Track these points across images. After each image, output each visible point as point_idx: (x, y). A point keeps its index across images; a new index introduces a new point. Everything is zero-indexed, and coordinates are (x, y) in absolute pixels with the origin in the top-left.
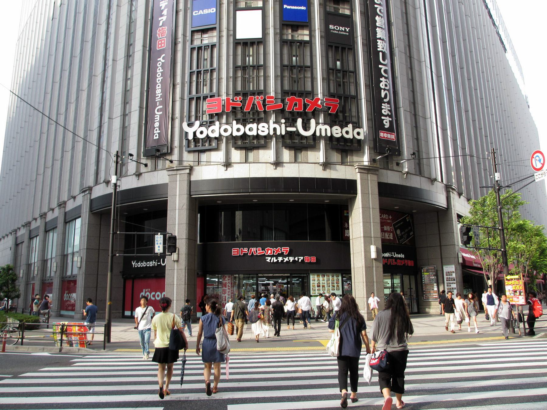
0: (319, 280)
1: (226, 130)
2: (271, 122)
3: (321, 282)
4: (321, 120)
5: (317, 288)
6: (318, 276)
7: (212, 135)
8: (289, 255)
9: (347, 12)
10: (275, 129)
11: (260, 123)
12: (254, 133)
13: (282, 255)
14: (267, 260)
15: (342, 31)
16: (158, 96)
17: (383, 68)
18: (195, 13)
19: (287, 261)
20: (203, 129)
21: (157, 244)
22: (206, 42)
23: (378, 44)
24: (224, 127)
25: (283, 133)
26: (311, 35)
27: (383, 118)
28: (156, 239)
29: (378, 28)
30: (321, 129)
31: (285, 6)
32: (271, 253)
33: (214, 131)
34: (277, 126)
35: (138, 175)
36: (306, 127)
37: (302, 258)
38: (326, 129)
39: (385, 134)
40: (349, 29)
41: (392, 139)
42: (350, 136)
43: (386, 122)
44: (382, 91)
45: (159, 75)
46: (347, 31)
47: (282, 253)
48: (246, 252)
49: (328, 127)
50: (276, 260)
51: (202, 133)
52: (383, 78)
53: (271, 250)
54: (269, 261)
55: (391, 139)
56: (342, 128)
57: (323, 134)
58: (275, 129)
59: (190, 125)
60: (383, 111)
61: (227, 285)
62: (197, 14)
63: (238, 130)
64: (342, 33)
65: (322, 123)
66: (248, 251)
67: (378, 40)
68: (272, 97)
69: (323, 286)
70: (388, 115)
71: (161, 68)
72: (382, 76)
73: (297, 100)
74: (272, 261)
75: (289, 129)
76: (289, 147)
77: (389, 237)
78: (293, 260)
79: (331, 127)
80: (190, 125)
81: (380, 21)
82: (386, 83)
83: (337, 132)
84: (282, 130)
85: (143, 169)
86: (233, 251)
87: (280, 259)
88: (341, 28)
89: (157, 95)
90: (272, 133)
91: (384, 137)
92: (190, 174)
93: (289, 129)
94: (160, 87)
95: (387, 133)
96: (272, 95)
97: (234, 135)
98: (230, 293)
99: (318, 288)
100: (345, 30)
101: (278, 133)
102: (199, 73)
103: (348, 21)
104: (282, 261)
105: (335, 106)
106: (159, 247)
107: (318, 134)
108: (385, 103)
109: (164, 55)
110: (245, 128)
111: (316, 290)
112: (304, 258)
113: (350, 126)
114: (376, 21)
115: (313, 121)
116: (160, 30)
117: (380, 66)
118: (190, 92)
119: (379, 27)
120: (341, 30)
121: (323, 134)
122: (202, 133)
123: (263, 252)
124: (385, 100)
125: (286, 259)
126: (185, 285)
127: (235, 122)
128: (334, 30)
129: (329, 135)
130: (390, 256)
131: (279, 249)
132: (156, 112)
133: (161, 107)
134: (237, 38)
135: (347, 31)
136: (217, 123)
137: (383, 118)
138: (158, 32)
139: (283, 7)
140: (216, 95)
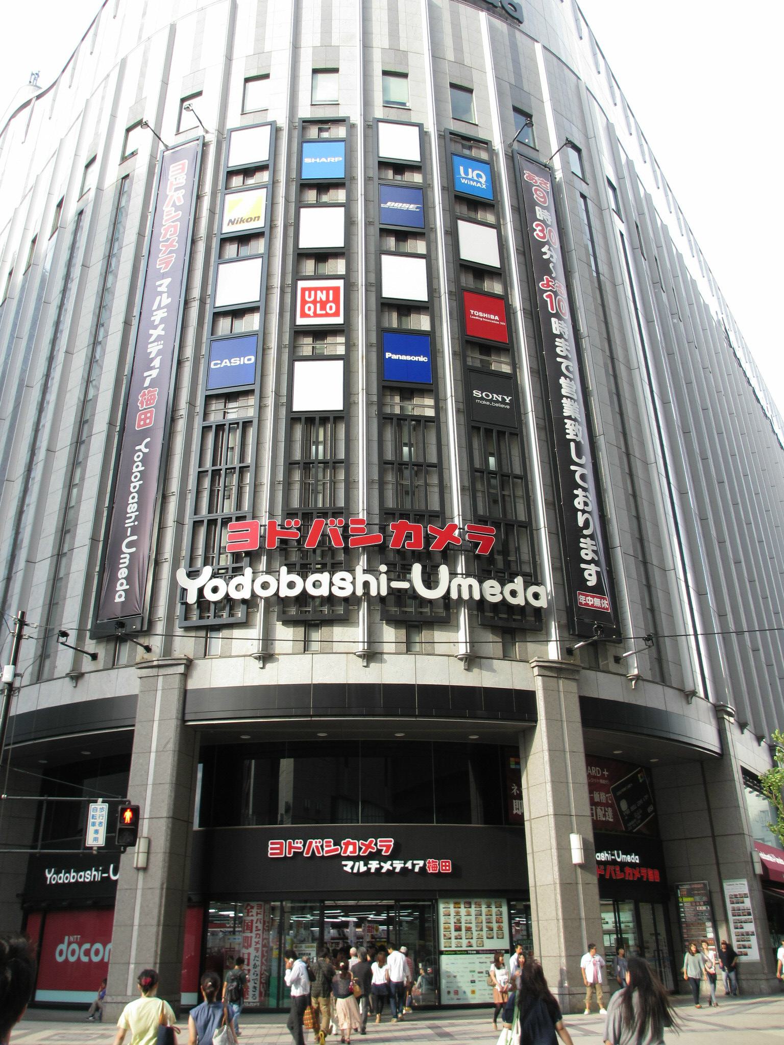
0: (458, 914)
1: (265, 586)
2: (359, 569)
3: (463, 919)
4: (461, 568)
5: (454, 934)
6: (457, 905)
8: (392, 857)
9: (506, 369)
10: (366, 585)
11: (337, 571)
12: (324, 591)
13: (376, 855)
14: (345, 868)
15: (497, 401)
16: (131, 517)
17: (579, 471)
18: (215, 364)
19: (388, 870)
21: (94, 824)
22: (232, 416)
25: (384, 592)
26: (439, 407)
27: (583, 566)
28: (91, 813)
29: (564, 398)
30: (460, 586)
31: (388, 355)
32: (354, 852)
34: (370, 578)
35: (76, 676)
36: (430, 581)
37: (421, 863)
38: (470, 586)
40: (510, 398)
41: (604, 608)
42: (519, 601)
43: (590, 575)
44: (579, 514)
45: (136, 477)
47: (379, 851)
48: (300, 848)
49: (474, 582)
51: (215, 590)
53: (354, 844)
54: (350, 871)
55: (601, 608)
56: (503, 585)
58: (366, 585)
59: (193, 574)
60: (583, 553)
61: (254, 925)
62: (219, 366)
63: (291, 585)
64: (497, 405)
65: (462, 574)
66: (304, 846)
67: (566, 421)
69: (468, 929)
72: (578, 486)
74: (355, 871)
75: (396, 585)
76: (395, 622)
77: (605, 815)
78: (402, 869)
79: (481, 582)
80: (193, 574)
81: (568, 386)
82: (586, 499)
83: (493, 591)
84: (380, 585)
85: (87, 664)
86: (270, 846)
87: (374, 865)
89: (128, 515)
90: (360, 592)
91: (587, 604)
92: (185, 676)
93: (396, 585)
94: (136, 500)
95: (593, 597)
96: (361, 517)
97: (282, 594)
98: (259, 946)
99: (457, 933)
101: (373, 592)
103: (510, 383)
106: (96, 832)
107: (454, 595)
108: (585, 537)
109: (148, 440)
110: (304, 581)
111: (453, 938)
112: (425, 865)
113: (519, 580)
114: (560, 387)
115: (444, 570)
116: (144, 395)
117: (573, 468)
118: (196, 511)
119: (567, 397)
120: (494, 399)
121: (466, 596)
122: (215, 590)
123: (337, 850)
124: (585, 532)
125: (387, 866)
126: (158, 925)
127: (284, 569)
128: (482, 399)
130: (609, 859)
132: (124, 549)
134: (295, 409)
135: (507, 401)
136: (248, 571)
137: (583, 566)
139: (385, 355)
140: (249, 516)
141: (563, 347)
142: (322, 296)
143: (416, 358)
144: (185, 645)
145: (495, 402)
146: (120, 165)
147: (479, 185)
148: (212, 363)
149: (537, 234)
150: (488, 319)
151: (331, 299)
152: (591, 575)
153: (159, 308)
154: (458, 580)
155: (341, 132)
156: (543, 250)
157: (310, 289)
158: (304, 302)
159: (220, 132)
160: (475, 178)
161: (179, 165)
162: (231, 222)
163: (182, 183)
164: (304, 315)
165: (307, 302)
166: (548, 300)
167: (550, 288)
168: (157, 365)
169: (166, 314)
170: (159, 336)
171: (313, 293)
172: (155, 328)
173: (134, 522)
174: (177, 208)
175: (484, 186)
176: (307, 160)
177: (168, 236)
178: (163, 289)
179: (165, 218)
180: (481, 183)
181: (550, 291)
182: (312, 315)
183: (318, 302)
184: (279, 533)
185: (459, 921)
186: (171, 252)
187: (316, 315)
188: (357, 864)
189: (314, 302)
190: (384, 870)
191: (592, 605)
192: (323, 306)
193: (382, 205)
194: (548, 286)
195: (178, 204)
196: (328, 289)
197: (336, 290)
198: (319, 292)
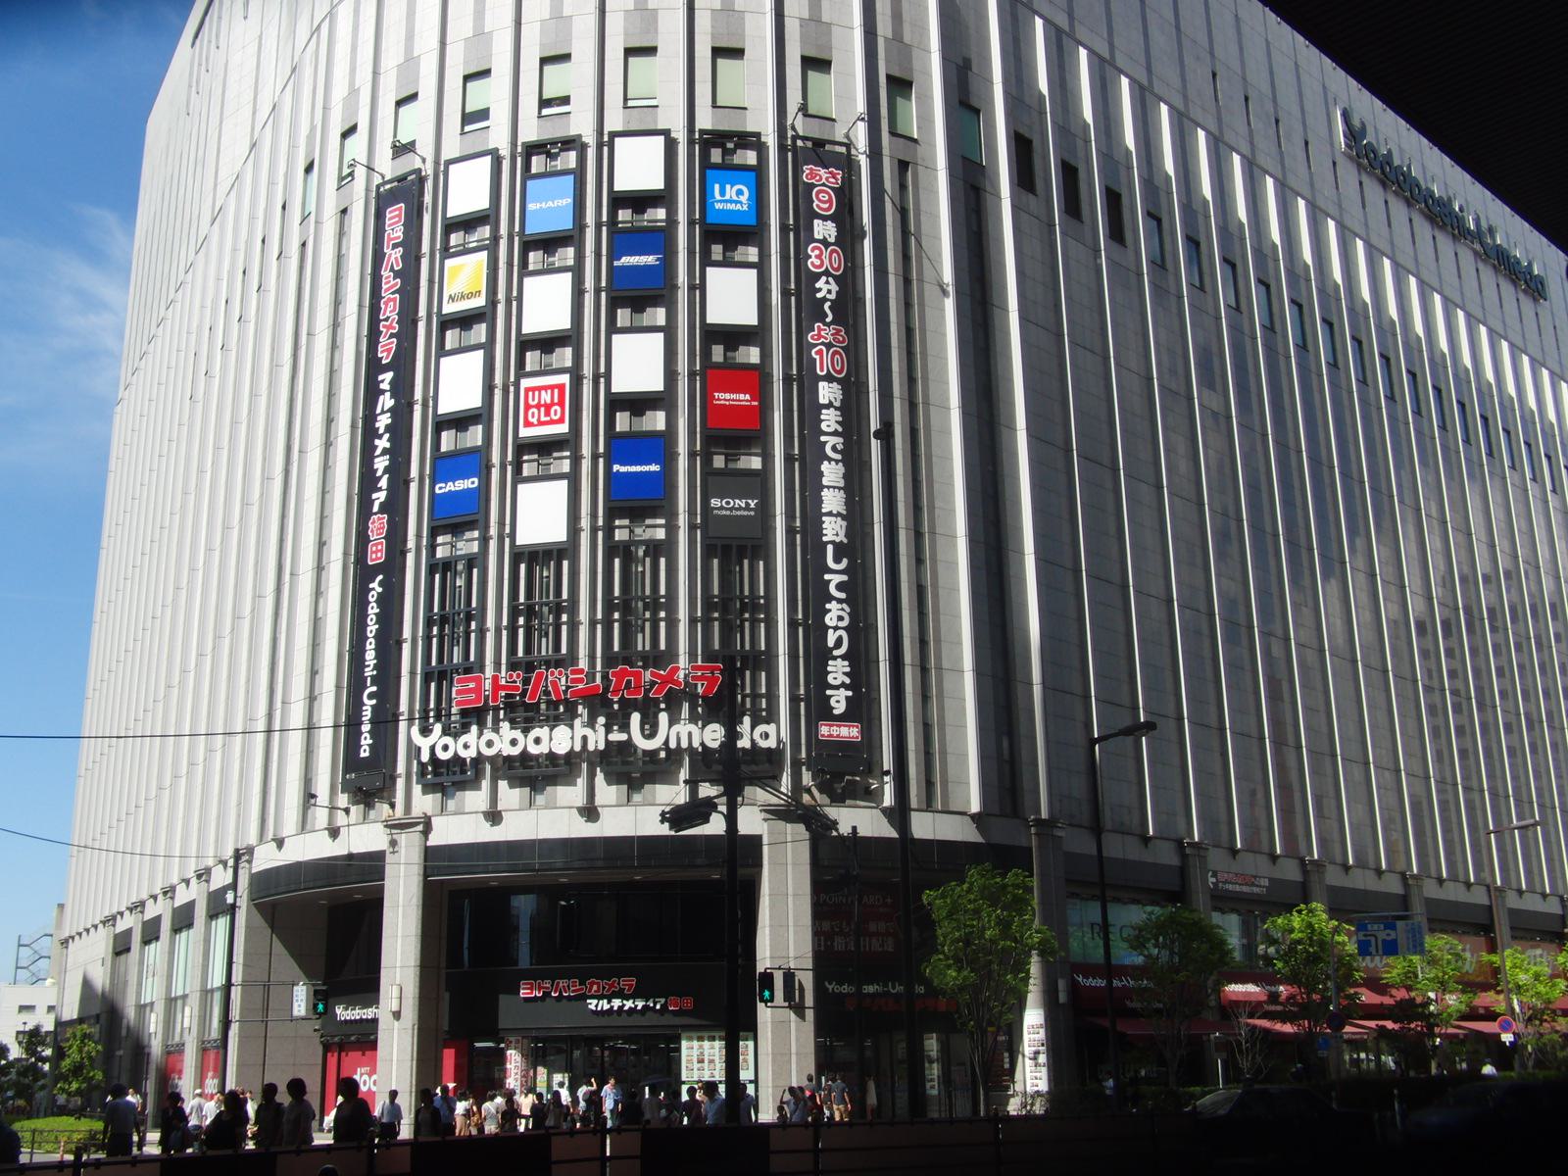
0: (701, 1047)
2: (577, 722)
3: (706, 1053)
5: (696, 1066)
7: (463, 754)
8: (633, 996)
9: (756, 463)
10: (585, 739)
12: (543, 749)
14: (590, 1006)
15: (740, 508)
16: (369, 666)
17: (834, 579)
18: (440, 488)
19: (630, 1008)
21: (297, 1001)
23: (824, 526)
24: (488, 735)
25: (602, 746)
29: (825, 490)
31: (616, 468)
33: (470, 744)
34: (588, 732)
35: (334, 832)
36: (650, 728)
38: (690, 734)
39: (835, 728)
40: (756, 501)
41: (853, 737)
43: (838, 702)
44: (831, 631)
45: (372, 620)
46: (752, 506)
47: (622, 990)
48: (548, 988)
50: (609, 1006)
51: (446, 748)
52: (834, 602)
53: (598, 984)
54: (594, 1009)
55: (850, 737)
57: (684, 744)
58: (585, 739)
59: (426, 731)
60: (830, 679)
61: (513, 1058)
62: (442, 491)
63: (514, 742)
64: (739, 513)
65: (685, 719)
66: (552, 986)
67: (824, 518)
68: (581, 671)
69: (711, 1061)
70: (843, 685)
71: (375, 605)
72: (831, 598)
74: (599, 1009)
76: (613, 778)
77: (882, 946)
78: (643, 1006)
80: (426, 731)
81: (832, 473)
82: (841, 613)
84: (597, 739)
86: (522, 986)
88: (737, 501)
89: (367, 663)
90: (578, 748)
91: (831, 736)
94: (373, 646)
95: (839, 726)
98: (519, 1077)
99: (700, 1065)
100: (747, 504)
101: (591, 747)
104: (621, 1008)
106: (299, 1006)
107: (673, 745)
108: (835, 658)
109: (380, 577)
110: (526, 737)
111: (695, 1069)
112: (666, 1001)
114: (821, 474)
115: (663, 717)
116: (374, 522)
117: (827, 577)
119: (828, 487)
120: (737, 506)
121: (684, 744)
122: (446, 748)
123: (582, 989)
124: (836, 653)
125: (629, 1004)
126: (412, 1060)
127: (505, 726)
128: (722, 508)
129: (696, 744)
131: (615, 981)
133: (374, 689)
135: (752, 506)
136: (474, 728)
137: (828, 692)
138: (370, 525)
141: (830, 420)
142: (546, 397)
143: (646, 468)
144: (424, 803)
145: (737, 509)
146: (337, 190)
147: (739, 207)
148: (437, 486)
149: (812, 263)
150: (736, 400)
151: (556, 401)
152: (839, 701)
153: (383, 412)
154: (676, 728)
155: (571, 159)
156: (817, 285)
157: (533, 389)
158: (528, 407)
159: (437, 163)
160: (735, 198)
161: (395, 210)
162: (452, 298)
163: (399, 237)
164: (528, 424)
166: (817, 357)
167: (822, 340)
168: (385, 487)
169: (389, 421)
170: (384, 449)
171: (537, 393)
172: (380, 437)
173: (372, 671)
174: (397, 274)
175: (745, 208)
176: (531, 207)
177: (388, 314)
178: (385, 386)
179: (384, 287)
180: (741, 203)
181: (822, 344)
182: (536, 423)
183: (542, 406)
184: (504, 688)
185: (702, 1054)
186: (392, 336)
187: (541, 423)
188: (601, 1002)
189: (538, 406)
190: (626, 1008)
191: (838, 736)
192: (548, 407)
193: (616, 263)
194: (820, 336)
195: (396, 268)
196: (552, 387)
197: (561, 387)
198: (543, 392)
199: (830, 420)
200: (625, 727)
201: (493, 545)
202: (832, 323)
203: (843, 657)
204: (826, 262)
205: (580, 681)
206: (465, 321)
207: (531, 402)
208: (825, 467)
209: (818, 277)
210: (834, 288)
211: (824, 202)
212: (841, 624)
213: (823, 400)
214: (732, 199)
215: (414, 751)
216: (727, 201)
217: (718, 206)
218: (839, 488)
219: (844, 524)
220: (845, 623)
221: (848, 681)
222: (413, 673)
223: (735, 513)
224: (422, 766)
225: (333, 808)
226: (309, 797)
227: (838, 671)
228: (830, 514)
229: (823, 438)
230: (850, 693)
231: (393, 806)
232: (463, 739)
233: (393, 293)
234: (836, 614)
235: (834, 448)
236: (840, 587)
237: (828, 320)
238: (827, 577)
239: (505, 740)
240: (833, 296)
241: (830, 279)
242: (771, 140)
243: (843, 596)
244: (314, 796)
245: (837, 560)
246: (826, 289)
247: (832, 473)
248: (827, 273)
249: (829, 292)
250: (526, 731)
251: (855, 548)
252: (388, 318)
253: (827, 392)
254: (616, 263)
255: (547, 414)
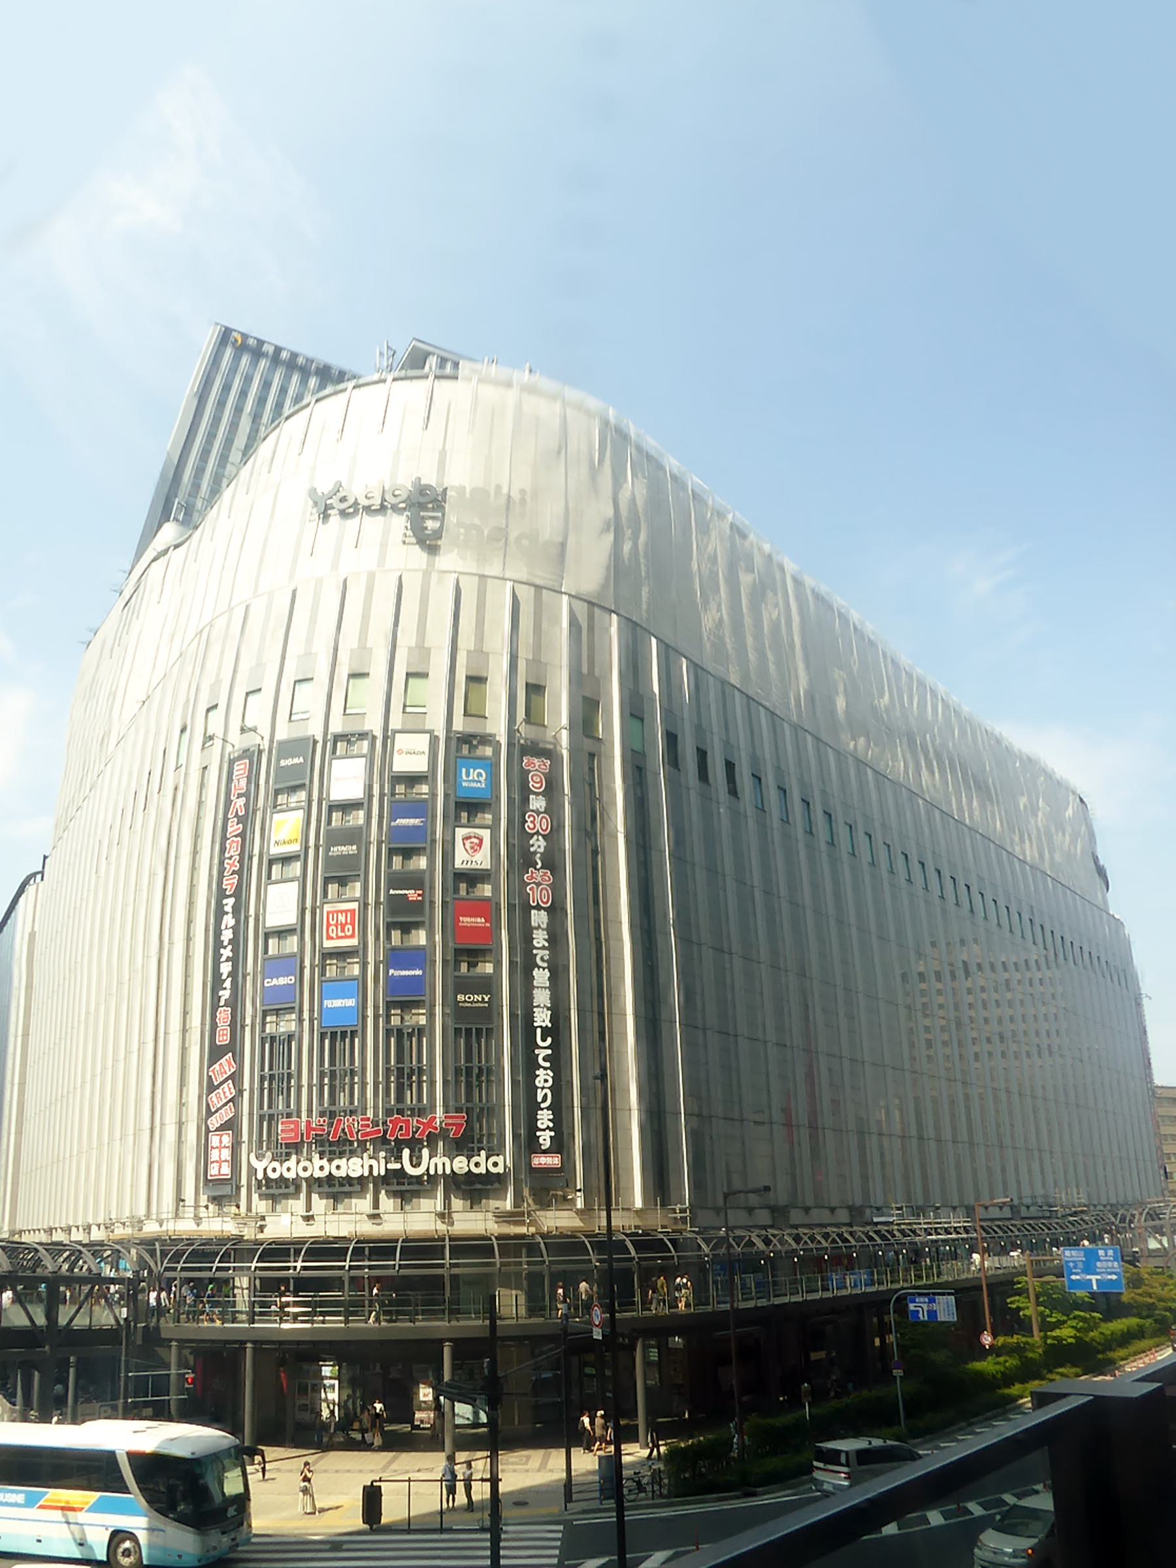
1: (305, 1169)
7: (287, 1175)
9: (489, 968)
10: (371, 1167)
17: (542, 1054)
20: (276, 1164)
22: (283, 1029)
25: (383, 1173)
27: (538, 1134)
30: (436, 1164)
31: (391, 972)
33: (292, 1168)
34: (374, 1162)
36: (416, 1162)
38: (444, 1164)
42: (482, 1170)
44: (539, 1091)
46: (486, 999)
51: (274, 1170)
52: (541, 1070)
56: (469, 1158)
57: (440, 1172)
58: (371, 1167)
59: (260, 1157)
63: (322, 1168)
64: (477, 1005)
67: (535, 1009)
68: (368, 1119)
73: (404, 1121)
75: (391, 1166)
76: (393, 1194)
80: (260, 1157)
81: (541, 977)
82: (547, 1077)
83: (461, 1165)
84: (380, 1169)
90: (366, 1174)
96: (368, 1116)
100: (483, 998)
101: (375, 1173)
102: (272, 1077)
103: (488, 985)
105: (460, 1125)
107: (432, 1172)
108: (542, 1109)
113: (483, 1153)
115: (425, 1152)
124: (543, 1105)
127: (316, 1156)
129: (448, 1171)
135: (486, 999)
136: (294, 1157)
137: (538, 1134)
140: (295, 1114)
141: (540, 939)
142: (342, 918)
143: (412, 973)
144: (261, 1206)
148: (266, 981)
151: (349, 921)
152: (545, 1138)
154: (434, 1160)
158: (329, 925)
160: (476, 778)
164: (329, 938)
165: (331, 925)
166: (531, 893)
175: (483, 786)
181: (534, 883)
182: (335, 936)
184: (314, 1130)
187: (338, 938)
193: (393, 824)
194: (533, 878)
196: (346, 911)
198: (340, 915)
199: (540, 939)
200: (399, 1158)
201: (306, 1024)
202: (541, 868)
203: (548, 1108)
204: (538, 826)
205: (368, 1126)
206: (286, 860)
207: (331, 922)
208: (536, 972)
209: (532, 836)
210: (542, 843)
211: (537, 783)
212: (547, 1085)
213: (534, 924)
214: (473, 779)
215: (252, 1171)
216: (470, 781)
217: (464, 784)
218: (545, 988)
219: (549, 1012)
220: (550, 1083)
221: (551, 1125)
222: (251, 1114)
223: (474, 1005)
224: (259, 1182)
225: (197, 1206)
226: (180, 1200)
227: (544, 1118)
228: (538, 1006)
229: (535, 952)
230: (553, 1134)
231: (238, 1207)
232: (286, 1164)
233: (236, 836)
234: (544, 1078)
235: (542, 959)
236: (544, 1059)
237: (538, 867)
238: (537, 1051)
239: (319, 1167)
240: (542, 850)
241: (540, 837)
242: (503, 739)
243: (548, 1064)
244: (183, 1201)
245: (544, 1040)
246: (538, 845)
247: (541, 977)
248: (537, 833)
249: (539, 847)
250: (330, 1161)
251: (556, 1031)
252: (232, 857)
253: (539, 918)
254: (393, 824)
255: (343, 931)
